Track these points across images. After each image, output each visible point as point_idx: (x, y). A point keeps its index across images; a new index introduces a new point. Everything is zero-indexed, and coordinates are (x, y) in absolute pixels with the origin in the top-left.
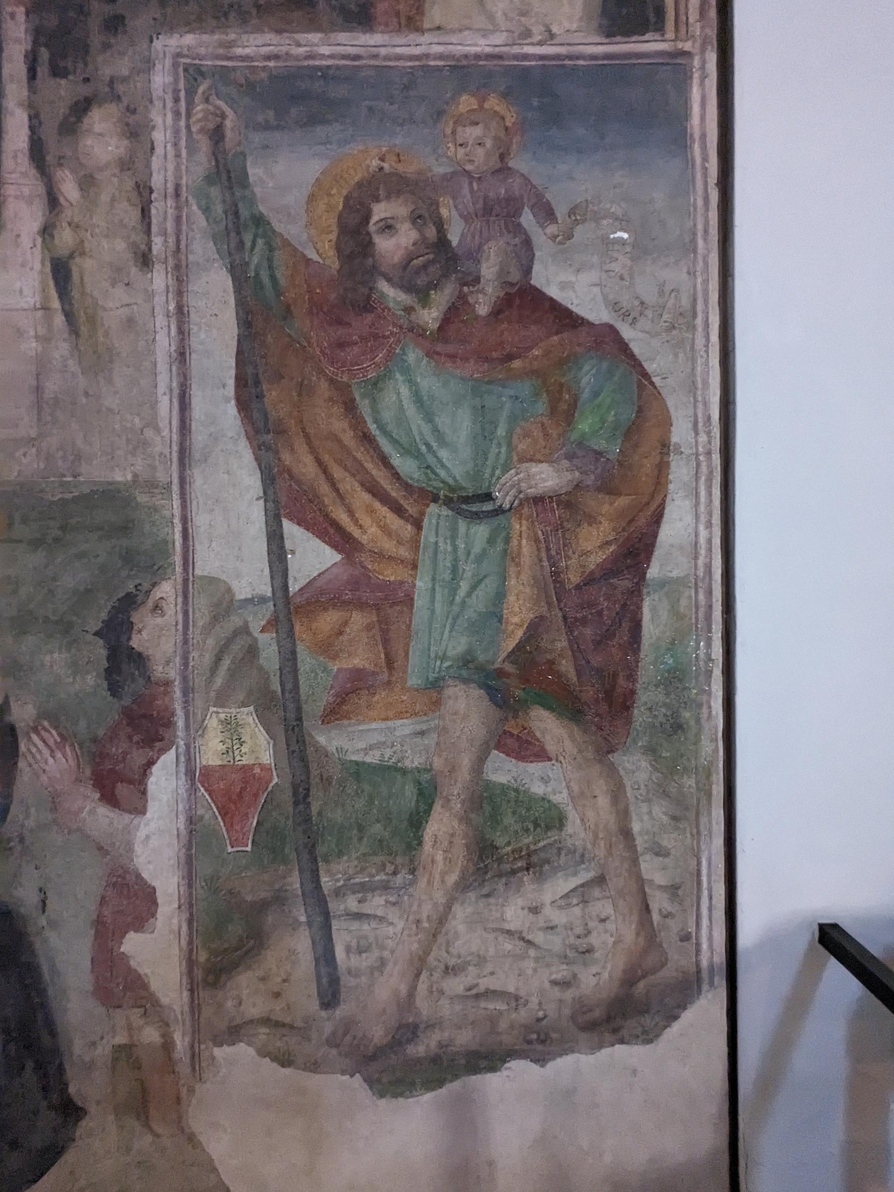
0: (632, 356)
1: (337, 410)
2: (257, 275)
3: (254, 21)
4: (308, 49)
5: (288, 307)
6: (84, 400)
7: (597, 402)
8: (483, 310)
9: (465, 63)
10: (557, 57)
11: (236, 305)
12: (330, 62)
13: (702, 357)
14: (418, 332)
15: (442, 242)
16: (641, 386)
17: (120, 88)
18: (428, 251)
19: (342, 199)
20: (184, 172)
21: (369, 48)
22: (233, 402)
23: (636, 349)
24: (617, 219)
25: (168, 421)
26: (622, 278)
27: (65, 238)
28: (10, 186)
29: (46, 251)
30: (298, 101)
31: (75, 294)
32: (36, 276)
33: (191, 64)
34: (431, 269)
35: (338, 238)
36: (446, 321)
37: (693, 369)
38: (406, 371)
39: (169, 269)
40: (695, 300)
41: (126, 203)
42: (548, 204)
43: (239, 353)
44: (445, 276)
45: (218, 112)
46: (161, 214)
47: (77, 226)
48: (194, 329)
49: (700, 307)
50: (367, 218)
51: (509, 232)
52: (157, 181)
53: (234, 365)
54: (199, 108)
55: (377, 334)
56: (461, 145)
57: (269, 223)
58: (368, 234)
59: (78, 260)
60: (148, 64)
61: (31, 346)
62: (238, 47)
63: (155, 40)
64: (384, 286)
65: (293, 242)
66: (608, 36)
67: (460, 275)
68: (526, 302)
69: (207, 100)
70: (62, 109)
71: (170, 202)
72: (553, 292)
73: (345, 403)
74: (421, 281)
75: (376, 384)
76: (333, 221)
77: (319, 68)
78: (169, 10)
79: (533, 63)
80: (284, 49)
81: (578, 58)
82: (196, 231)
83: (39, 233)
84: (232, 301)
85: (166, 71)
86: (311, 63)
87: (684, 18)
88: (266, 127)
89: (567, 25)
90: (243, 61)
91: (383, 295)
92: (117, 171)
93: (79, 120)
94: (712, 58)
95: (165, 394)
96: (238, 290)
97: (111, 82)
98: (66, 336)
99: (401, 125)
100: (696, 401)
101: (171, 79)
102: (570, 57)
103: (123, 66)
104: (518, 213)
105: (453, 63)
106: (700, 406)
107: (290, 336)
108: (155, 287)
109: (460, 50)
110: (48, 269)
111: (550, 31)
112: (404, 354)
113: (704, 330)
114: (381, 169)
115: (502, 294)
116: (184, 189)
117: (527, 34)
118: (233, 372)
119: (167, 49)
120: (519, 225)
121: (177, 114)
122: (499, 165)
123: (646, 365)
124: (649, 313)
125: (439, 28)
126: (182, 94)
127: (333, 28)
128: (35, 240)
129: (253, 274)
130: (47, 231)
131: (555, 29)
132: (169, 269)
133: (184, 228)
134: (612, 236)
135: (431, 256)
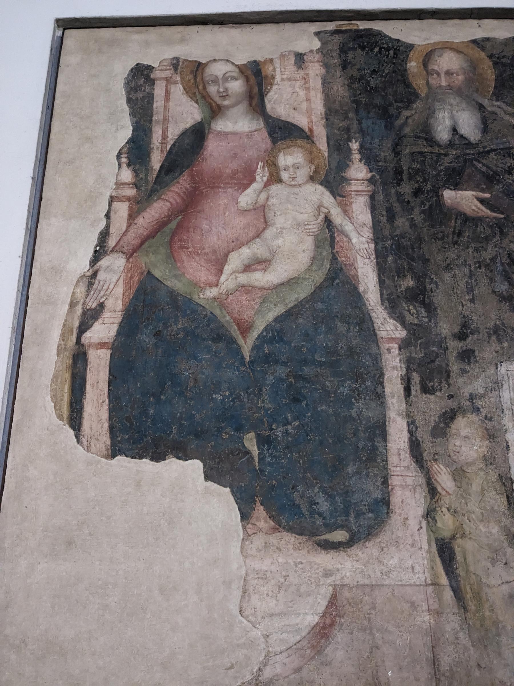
6: (477, 673)
17: (479, 403)
27: (446, 522)
28: (397, 478)
29: (431, 533)
31: (461, 571)
32: (424, 554)
41: (494, 493)
47: (455, 512)
59: (459, 541)
61: (425, 619)
63: (499, 366)
78: (505, 345)
83: (423, 517)
85: (511, 389)
93: (447, 426)
97: (472, 397)
98: (455, 610)
103: (478, 386)
110: (434, 548)
119: (509, 373)
128: (421, 522)
130: (430, 515)
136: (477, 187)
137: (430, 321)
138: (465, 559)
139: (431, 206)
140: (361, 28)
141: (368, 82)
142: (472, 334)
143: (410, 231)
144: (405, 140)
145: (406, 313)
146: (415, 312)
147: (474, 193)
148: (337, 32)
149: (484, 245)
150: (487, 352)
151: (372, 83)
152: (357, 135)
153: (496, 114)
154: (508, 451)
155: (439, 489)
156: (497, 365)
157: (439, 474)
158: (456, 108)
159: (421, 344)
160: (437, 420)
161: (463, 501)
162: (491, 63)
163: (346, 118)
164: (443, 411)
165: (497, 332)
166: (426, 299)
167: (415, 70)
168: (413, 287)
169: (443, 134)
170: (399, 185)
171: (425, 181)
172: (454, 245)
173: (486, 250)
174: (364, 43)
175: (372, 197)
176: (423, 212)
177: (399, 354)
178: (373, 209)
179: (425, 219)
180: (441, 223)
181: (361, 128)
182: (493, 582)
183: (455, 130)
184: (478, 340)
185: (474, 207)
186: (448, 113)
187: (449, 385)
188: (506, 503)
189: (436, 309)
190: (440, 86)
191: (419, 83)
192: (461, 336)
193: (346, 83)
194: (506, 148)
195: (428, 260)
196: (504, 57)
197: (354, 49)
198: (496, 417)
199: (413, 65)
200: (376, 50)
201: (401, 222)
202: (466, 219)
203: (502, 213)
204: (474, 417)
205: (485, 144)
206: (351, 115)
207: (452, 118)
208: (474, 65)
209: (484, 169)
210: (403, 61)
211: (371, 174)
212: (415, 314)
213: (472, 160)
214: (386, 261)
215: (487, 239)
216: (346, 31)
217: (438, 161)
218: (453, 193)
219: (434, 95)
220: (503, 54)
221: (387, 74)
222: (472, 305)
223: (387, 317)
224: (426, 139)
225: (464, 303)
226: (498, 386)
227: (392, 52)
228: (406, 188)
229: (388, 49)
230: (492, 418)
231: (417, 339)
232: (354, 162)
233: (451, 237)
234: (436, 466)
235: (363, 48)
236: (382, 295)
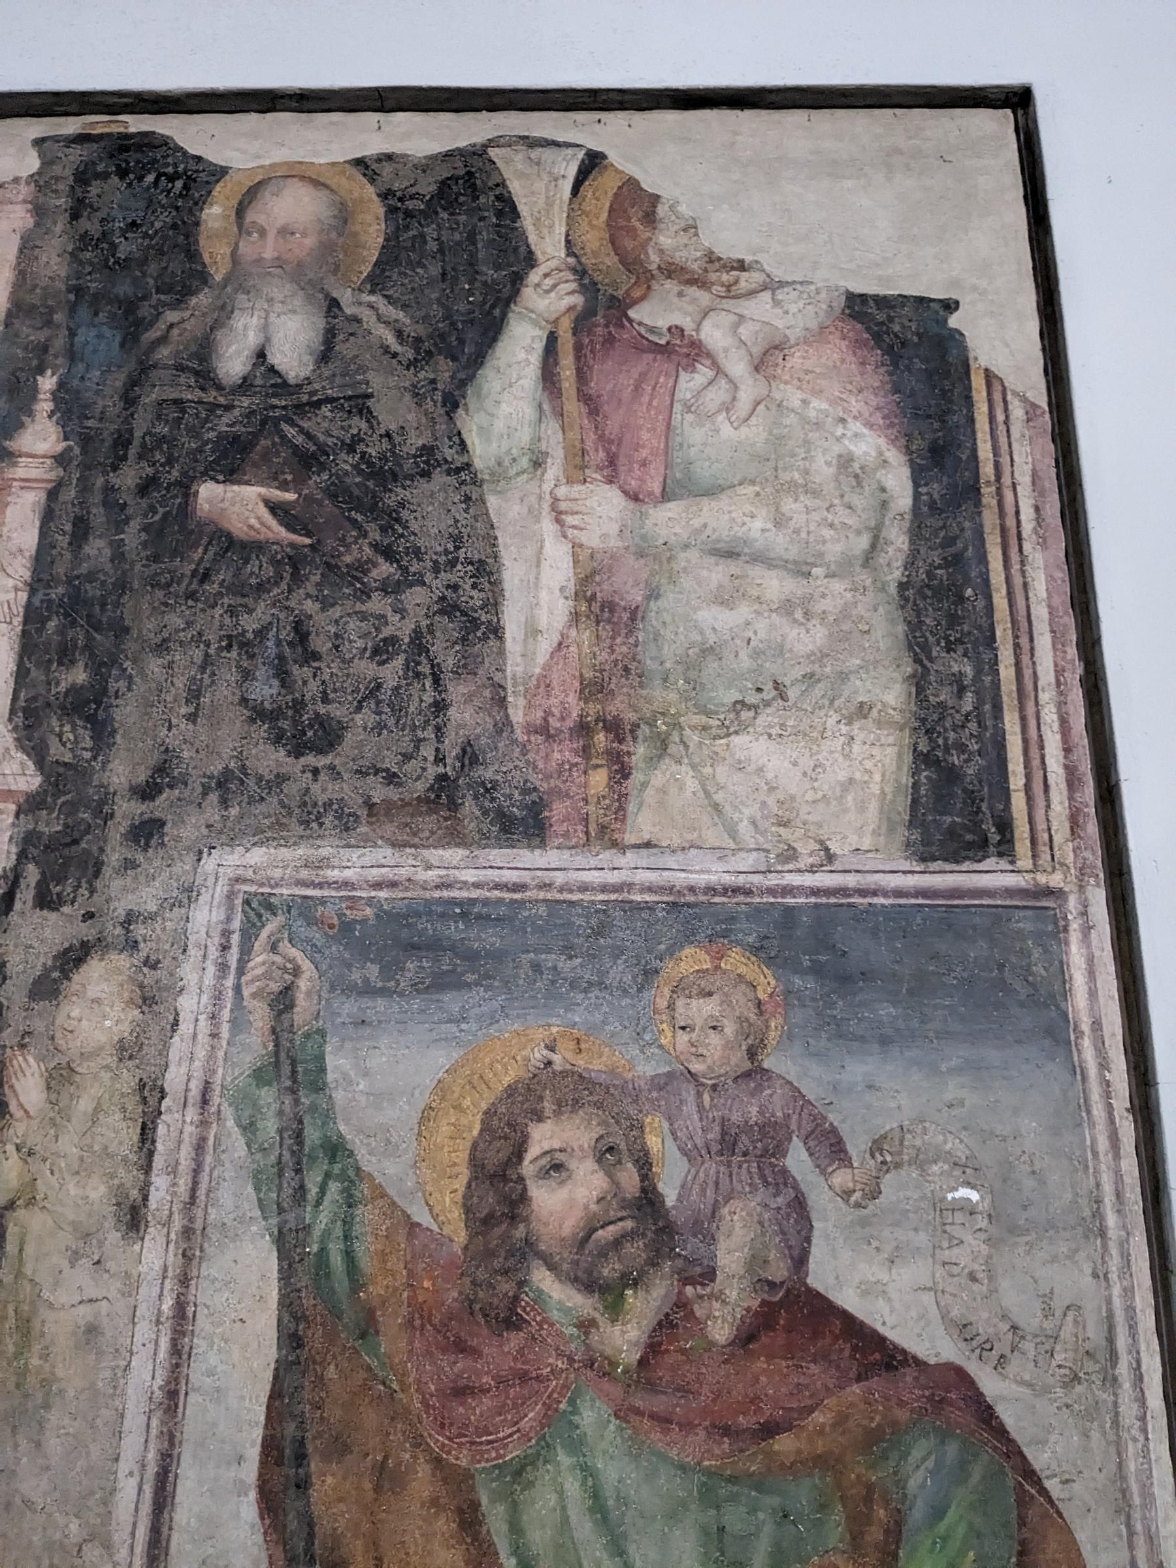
0: (1001, 1432)
1: (445, 1525)
2: (323, 1250)
3: (363, 829)
4: (443, 872)
5: (370, 1314)
7: (942, 1527)
8: (721, 1332)
9: (691, 899)
10: (842, 891)
11: (281, 1304)
12: (475, 894)
13: (1135, 1440)
14: (598, 1366)
15: (648, 1201)
16: (1023, 1500)
17: (139, 931)
18: (624, 1214)
19: (479, 1117)
20: (220, 1062)
21: (539, 873)
22: (253, 1495)
23: (1007, 1415)
24: (955, 1164)
25: (130, 1529)
26: (973, 1278)
30: (418, 951)
33: (256, 894)
34: (629, 1249)
35: (469, 1186)
36: (653, 1350)
37: (1120, 1465)
38: (576, 1445)
39: (173, 1236)
40: (1111, 1328)
41: (118, 1116)
42: (834, 1131)
43: (275, 1395)
44: (653, 1263)
45: (289, 966)
46: (174, 1134)
48: (200, 1344)
49: (1122, 1342)
50: (519, 1153)
51: (767, 1184)
52: (174, 1079)
53: (262, 1419)
54: (259, 959)
55: (526, 1372)
56: (683, 1028)
57: (351, 1154)
58: (521, 1179)
59: (21, 1213)
60: (190, 893)
62: (334, 867)
63: (205, 855)
64: (542, 1279)
65: (391, 1192)
66: (923, 860)
67: (680, 1263)
68: (798, 1317)
69: (274, 948)
70: (42, 958)
71: (192, 1114)
72: (848, 1299)
73: (460, 1511)
74: (609, 1270)
75: (519, 1473)
76: (463, 1156)
77: (454, 902)
78: (234, 811)
79: (802, 900)
80: (404, 872)
81: (875, 893)
82: (227, 1165)
84: (274, 1296)
85: (215, 903)
86: (446, 894)
87: (1046, 836)
88: (367, 990)
89: (853, 840)
90: (339, 889)
91: (540, 1297)
92: (112, 1061)
94: (1098, 898)
95: (131, 1474)
96: (286, 1275)
97: (130, 919)
99: (585, 991)
100: (1131, 1534)
101: (222, 917)
102: (862, 892)
103: (147, 897)
104: (781, 1150)
105: (671, 899)
106: (1140, 1541)
107: (369, 1369)
108: (143, 1269)
109: (680, 879)
111: (827, 849)
112: (575, 1411)
113: (1135, 1386)
114: (549, 1063)
115: (755, 1304)
116: (218, 1089)
117: (790, 854)
118: (258, 1434)
119: (221, 869)
120: (784, 1172)
121: (223, 968)
122: (747, 1065)
123: (1026, 1451)
124: (1028, 1346)
125: (648, 845)
126: (235, 939)
127: (484, 840)
129: (315, 1248)
131: (834, 847)
132: (173, 1236)
133: (209, 1159)
134: (950, 1196)
135: (629, 1224)
136: (275, 479)
137: (95, 758)
138: (21, 1250)
139: (166, 516)
140: (132, 130)
141: (114, 247)
142: (171, 787)
143: (108, 566)
144: (154, 374)
145: (53, 742)
146: (72, 737)
147: (262, 490)
148: (82, 139)
149: (249, 601)
150: (187, 829)
151: (122, 248)
152: (60, 361)
153: (358, 321)
154: (174, 1031)
155: (13, 1107)
156: (200, 852)
157: (19, 1074)
158: (278, 307)
159: (64, 803)
160: (49, 963)
161: (52, 1132)
162: (381, 211)
163: (49, 323)
164: (66, 945)
165: (225, 785)
166: (100, 712)
167: (216, 225)
168: (82, 687)
169: (233, 363)
170: (115, 468)
171: (170, 461)
172: (187, 598)
173: (250, 611)
174: (128, 163)
175: (53, 495)
176: (146, 528)
177: (13, 824)
178: (48, 516)
179: (145, 545)
180: (174, 553)
181: (72, 345)
182: (63, 1297)
183: (261, 355)
184: (179, 799)
185: (253, 521)
186: (259, 317)
187: (92, 891)
188: (136, 1138)
189: (115, 731)
190: (259, 261)
191: (215, 252)
192: (147, 792)
193: (70, 249)
194: (357, 397)
195: (127, 630)
196: (412, 198)
197: (105, 176)
198: (166, 962)
199: (215, 214)
200: (150, 178)
201: (97, 548)
202: (231, 546)
203: (309, 534)
204: (122, 961)
205: (317, 386)
206: (58, 317)
207: (265, 327)
208: (344, 215)
209: (300, 440)
210: (196, 204)
211: (65, 444)
212: (67, 740)
213: (277, 421)
214: (40, 631)
215: (261, 588)
216: (101, 137)
217: (207, 420)
218: (220, 488)
219: (240, 278)
220: (413, 190)
221: (156, 232)
222: (191, 727)
223: (12, 747)
224: (197, 373)
225: (174, 721)
226: (189, 898)
227: (179, 184)
228: (128, 477)
229: (172, 178)
230: (158, 962)
231: (58, 793)
232: (38, 418)
233: (186, 581)
234: (20, 1059)
235: (122, 173)
236: (15, 699)
